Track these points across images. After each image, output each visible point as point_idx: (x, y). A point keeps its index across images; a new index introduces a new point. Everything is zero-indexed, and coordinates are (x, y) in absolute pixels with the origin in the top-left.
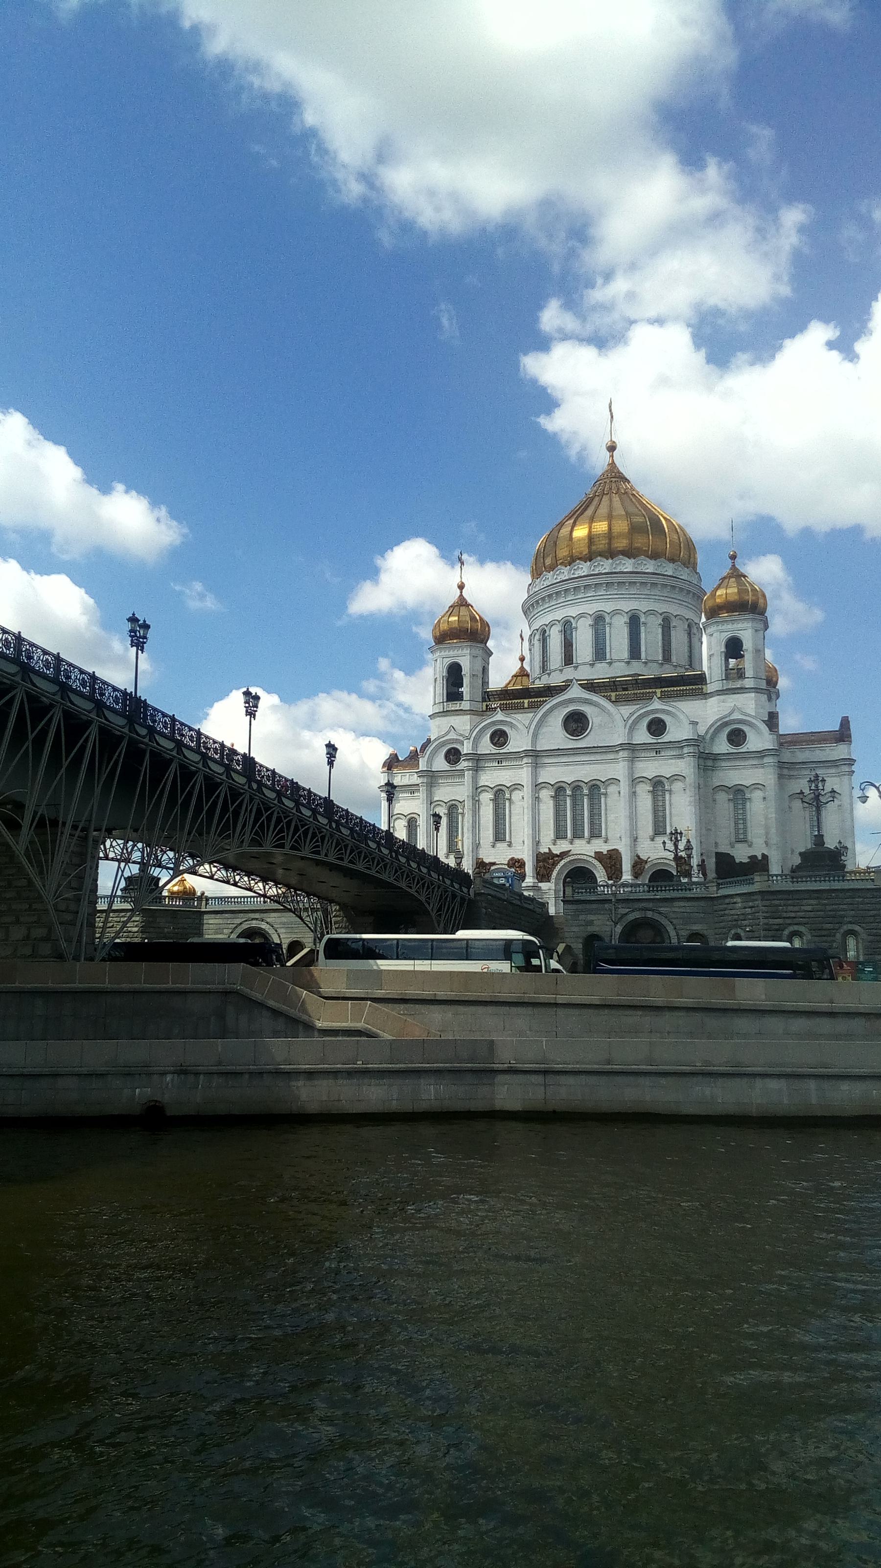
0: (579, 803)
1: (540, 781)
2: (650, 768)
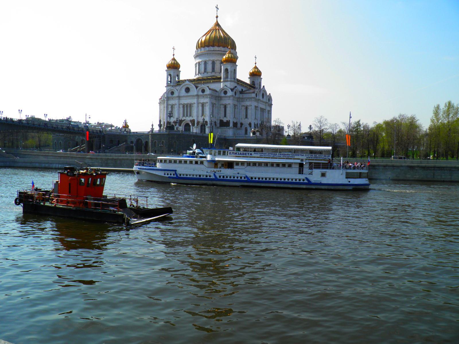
1: (180, 103)
2: (202, 100)
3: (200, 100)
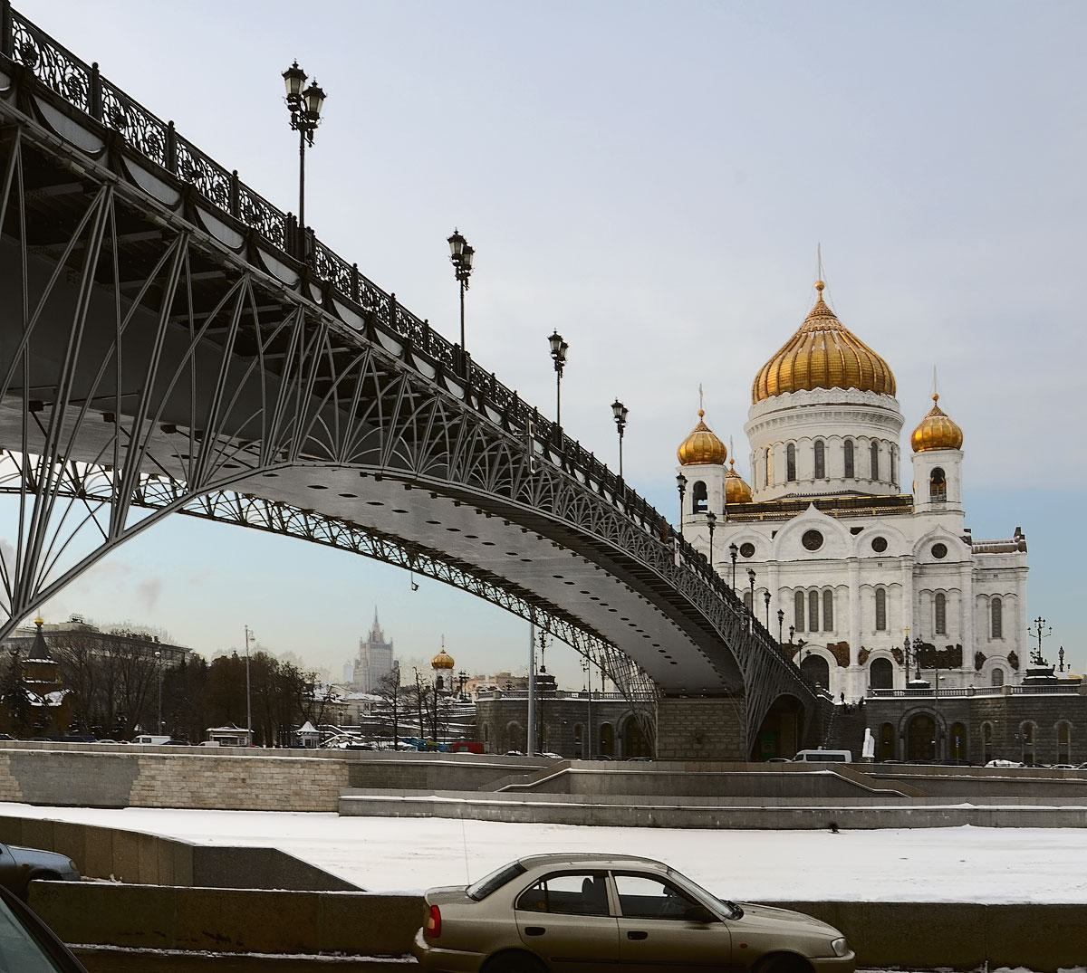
0: (816, 605)
2: (875, 577)
3: (864, 574)
